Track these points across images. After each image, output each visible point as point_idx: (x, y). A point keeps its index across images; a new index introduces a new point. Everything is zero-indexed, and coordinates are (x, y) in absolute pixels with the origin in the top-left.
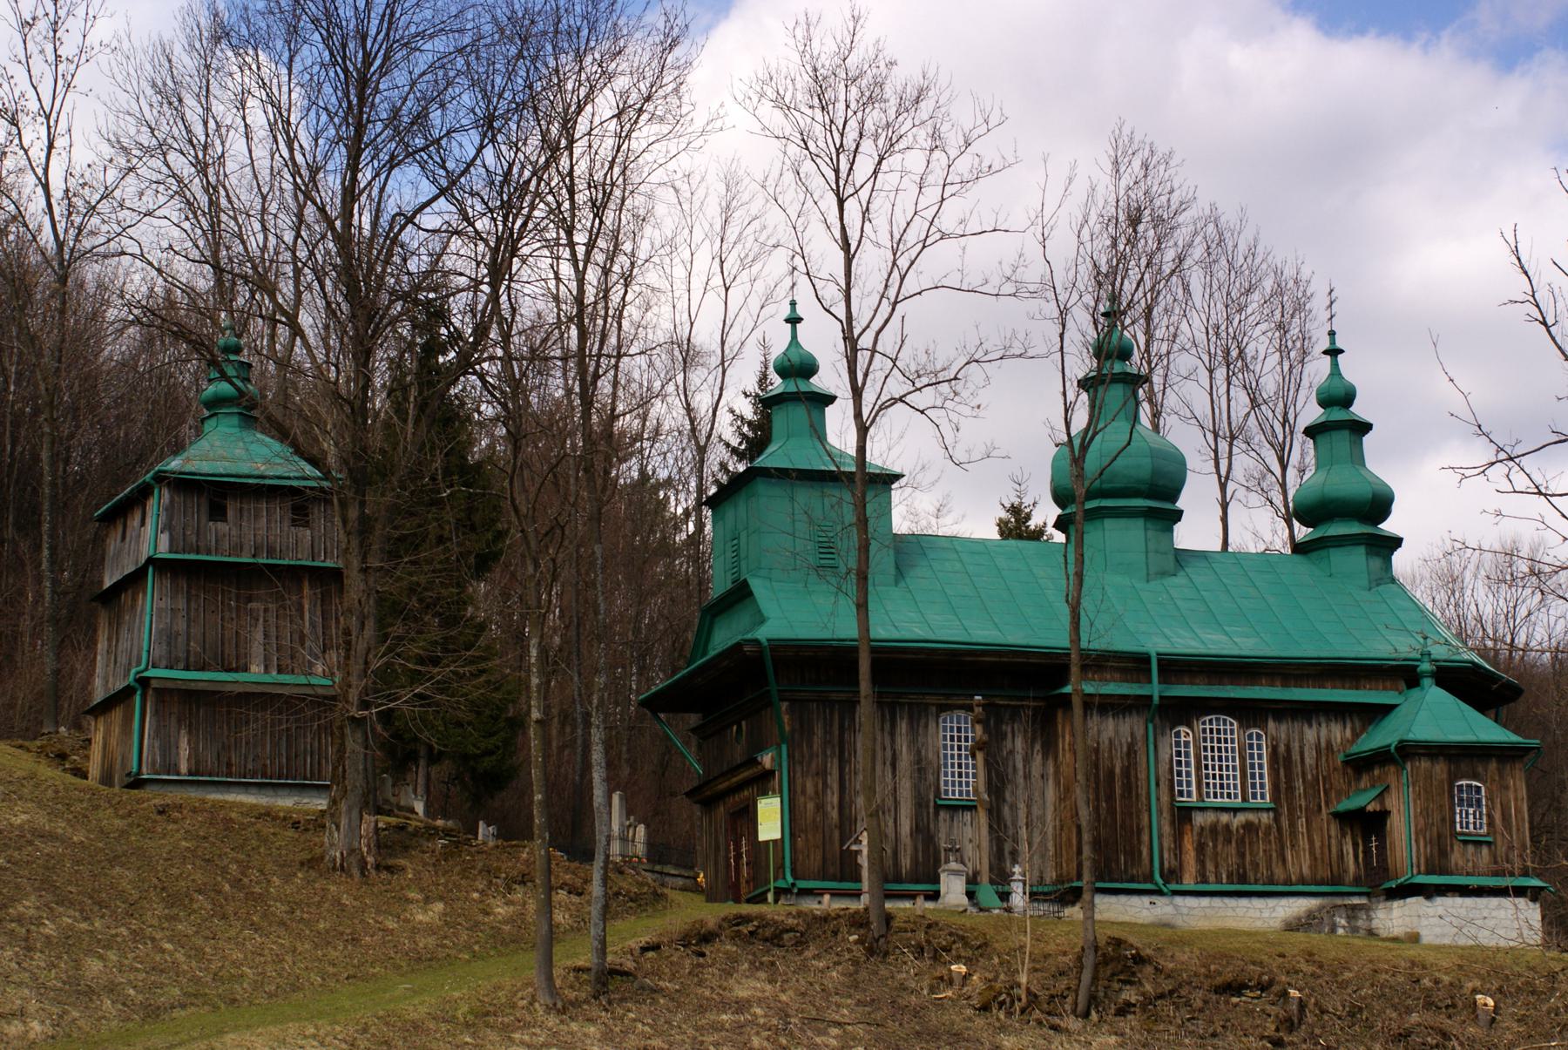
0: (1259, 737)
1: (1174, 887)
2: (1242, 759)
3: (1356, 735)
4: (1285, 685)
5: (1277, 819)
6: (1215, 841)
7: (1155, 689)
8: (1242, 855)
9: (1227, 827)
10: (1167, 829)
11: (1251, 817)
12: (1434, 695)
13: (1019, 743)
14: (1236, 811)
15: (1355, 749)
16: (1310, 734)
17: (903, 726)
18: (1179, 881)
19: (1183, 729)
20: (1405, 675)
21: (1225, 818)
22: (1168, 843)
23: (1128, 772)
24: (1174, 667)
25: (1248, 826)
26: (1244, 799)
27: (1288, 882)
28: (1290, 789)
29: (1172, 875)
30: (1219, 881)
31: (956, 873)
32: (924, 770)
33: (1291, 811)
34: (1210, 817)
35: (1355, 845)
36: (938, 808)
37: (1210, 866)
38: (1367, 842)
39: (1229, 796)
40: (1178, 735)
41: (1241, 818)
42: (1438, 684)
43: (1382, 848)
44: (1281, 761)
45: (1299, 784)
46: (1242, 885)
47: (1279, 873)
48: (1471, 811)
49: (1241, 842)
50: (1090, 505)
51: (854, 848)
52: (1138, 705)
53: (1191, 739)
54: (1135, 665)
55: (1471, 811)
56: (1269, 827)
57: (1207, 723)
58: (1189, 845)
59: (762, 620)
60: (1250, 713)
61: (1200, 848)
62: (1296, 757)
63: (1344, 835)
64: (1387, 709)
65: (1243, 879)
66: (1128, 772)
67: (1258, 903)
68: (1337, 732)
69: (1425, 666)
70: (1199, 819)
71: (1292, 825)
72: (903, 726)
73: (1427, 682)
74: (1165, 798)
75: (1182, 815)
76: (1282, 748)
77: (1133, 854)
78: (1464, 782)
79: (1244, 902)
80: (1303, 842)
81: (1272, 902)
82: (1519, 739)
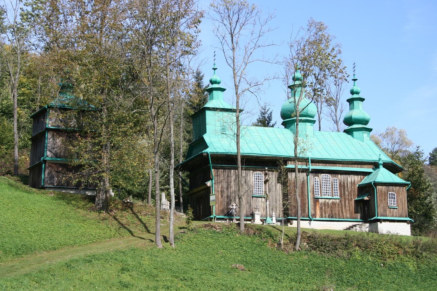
0: (336, 180)
1: (314, 219)
2: (332, 186)
3: (361, 180)
5: (341, 201)
6: (325, 206)
8: (332, 211)
10: (312, 203)
11: (334, 200)
12: (382, 169)
14: (330, 199)
15: (361, 183)
18: (316, 218)
19: (317, 177)
20: (376, 165)
21: (327, 200)
22: (313, 207)
24: (314, 161)
25: (333, 203)
26: (332, 196)
28: (345, 194)
29: (314, 215)
30: (325, 217)
31: (258, 214)
33: (345, 199)
34: (323, 200)
35: (361, 209)
36: (253, 197)
37: (323, 214)
38: (364, 208)
39: (328, 195)
40: (315, 179)
42: (383, 167)
43: (368, 210)
44: (342, 186)
45: (347, 193)
46: (332, 218)
47: (341, 215)
48: (392, 200)
49: (331, 207)
50: (300, 118)
51: (231, 207)
53: (318, 180)
54: (305, 160)
55: (392, 200)
56: (339, 204)
58: (318, 208)
59: (207, 147)
61: (321, 209)
63: (358, 206)
64: (369, 173)
65: (332, 217)
68: (356, 178)
69: (381, 162)
70: (320, 201)
73: (381, 167)
74: (312, 196)
75: (316, 200)
76: (342, 183)
78: (391, 193)
82: (405, 182)
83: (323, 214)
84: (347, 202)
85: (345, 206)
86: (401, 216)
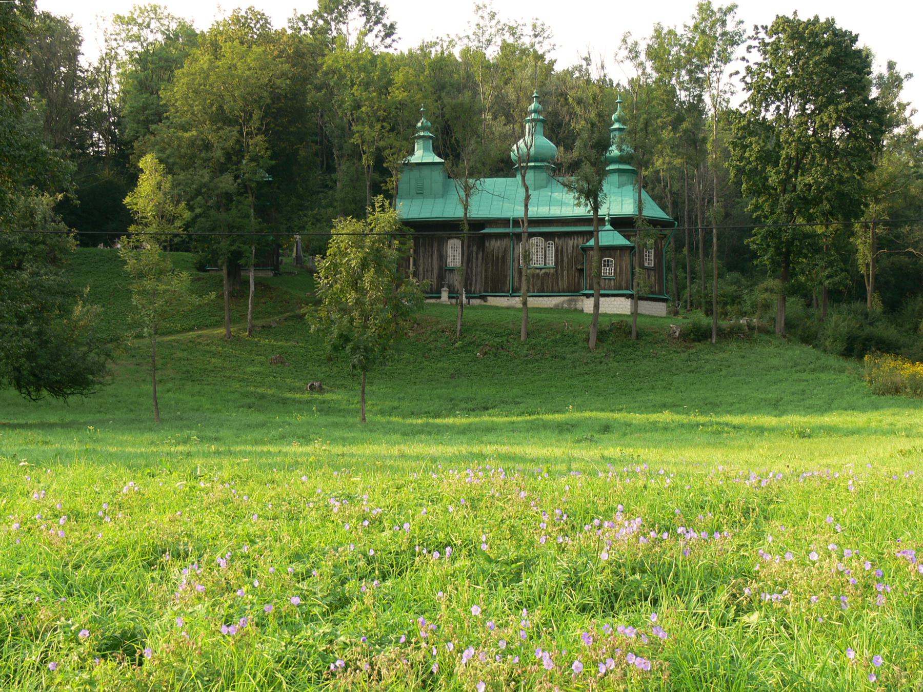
4: (562, 226)
7: (511, 230)
8: (542, 284)
9: (538, 274)
13: (475, 248)
14: (541, 269)
16: (570, 242)
17: (435, 245)
21: (538, 271)
23: (503, 257)
25: (545, 274)
27: (559, 292)
28: (562, 261)
32: (442, 258)
33: (562, 267)
37: (531, 287)
41: (543, 271)
44: (559, 253)
45: (565, 259)
47: (556, 288)
52: (505, 235)
57: (534, 240)
60: (547, 236)
61: (528, 281)
62: (565, 250)
66: (503, 257)
67: (545, 299)
68: (580, 241)
71: (562, 273)
72: (435, 245)
77: (504, 283)
79: (541, 299)
80: (565, 278)
81: (550, 298)
83: (531, 287)
84: (565, 272)
85: (562, 276)
86: (620, 289)
